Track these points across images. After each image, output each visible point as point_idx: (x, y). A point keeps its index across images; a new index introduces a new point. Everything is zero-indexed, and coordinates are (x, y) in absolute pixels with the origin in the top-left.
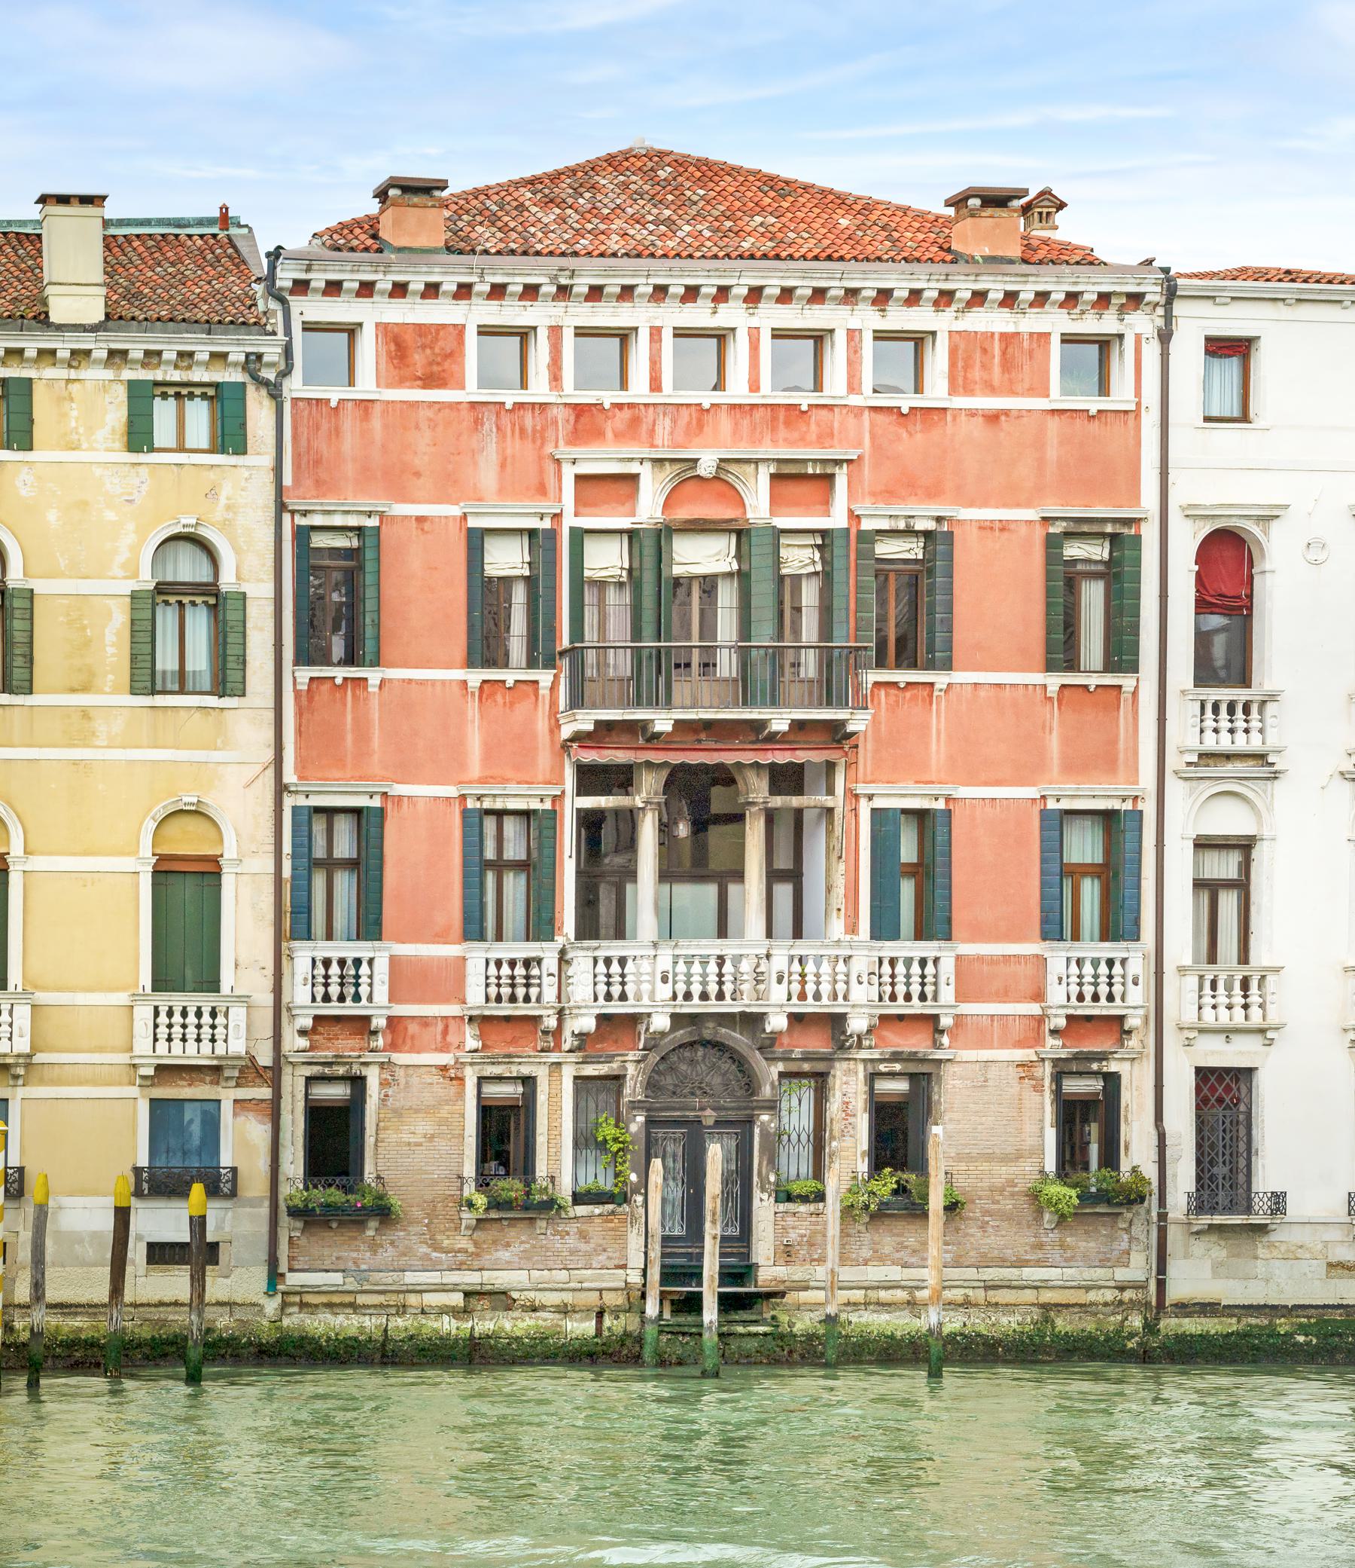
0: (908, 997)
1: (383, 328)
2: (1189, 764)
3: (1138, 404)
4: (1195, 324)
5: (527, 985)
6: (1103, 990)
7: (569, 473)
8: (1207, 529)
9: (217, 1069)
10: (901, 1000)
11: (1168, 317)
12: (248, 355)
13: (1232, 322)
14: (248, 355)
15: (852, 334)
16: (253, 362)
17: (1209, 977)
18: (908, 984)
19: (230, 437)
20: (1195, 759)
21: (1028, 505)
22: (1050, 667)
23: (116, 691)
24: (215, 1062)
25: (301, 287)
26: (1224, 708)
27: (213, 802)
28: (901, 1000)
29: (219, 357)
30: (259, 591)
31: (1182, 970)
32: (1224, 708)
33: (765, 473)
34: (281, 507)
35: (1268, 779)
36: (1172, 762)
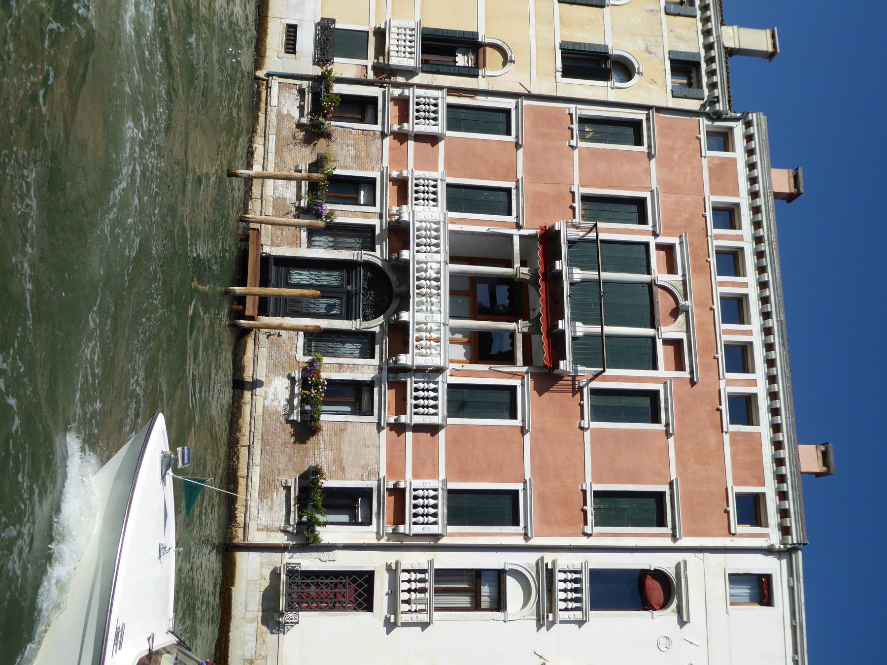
0: (416, 398)
1: (734, 160)
2: (547, 565)
3: (734, 535)
5: (424, 199)
6: (420, 510)
7: (675, 240)
8: (672, 573)
9: (383, 54)
10: (415, 394)
12: (718, 97)
14: (718, 97)
15: (754, 383)
16: (713, 101)
17: (427, 576)
18: (423, 398)
20: (550, 567)
21: (678, 473)
23: (561, 35)
24: (387, 51)
25: (748, 124)
26: (578, 585)
27: (509, 66)
28: (415, 394)
29: (713, 86)
31: (431, 562)
32: (578, 585)
33: (683, 336)
34: (647, 108)
35: (538, 615)
36: (549, 557)
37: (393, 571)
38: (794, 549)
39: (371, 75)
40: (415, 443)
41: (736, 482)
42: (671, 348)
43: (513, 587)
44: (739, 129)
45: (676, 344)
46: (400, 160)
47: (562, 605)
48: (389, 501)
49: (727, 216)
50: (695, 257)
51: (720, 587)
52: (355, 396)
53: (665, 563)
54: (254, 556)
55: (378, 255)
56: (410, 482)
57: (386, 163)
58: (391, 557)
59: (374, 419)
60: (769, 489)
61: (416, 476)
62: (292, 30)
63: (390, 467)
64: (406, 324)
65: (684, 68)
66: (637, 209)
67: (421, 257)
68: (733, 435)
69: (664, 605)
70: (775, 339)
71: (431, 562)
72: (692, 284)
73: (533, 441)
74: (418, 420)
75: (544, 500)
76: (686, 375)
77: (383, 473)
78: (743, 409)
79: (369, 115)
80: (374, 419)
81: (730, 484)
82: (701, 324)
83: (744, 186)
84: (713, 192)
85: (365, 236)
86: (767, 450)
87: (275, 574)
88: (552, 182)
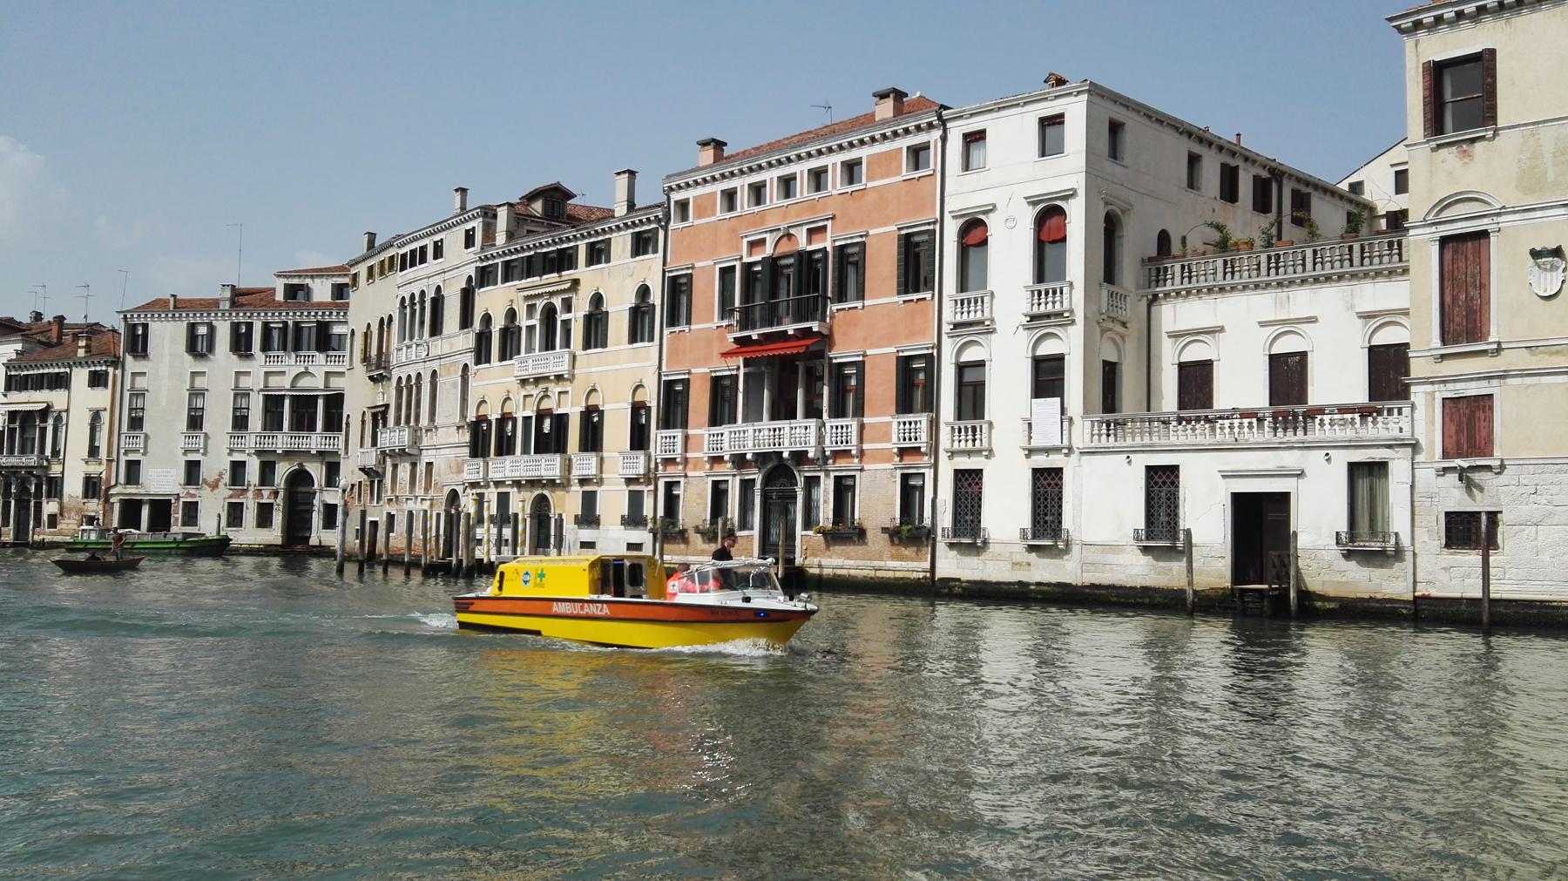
4: (956, 132)
8: (961, 221)
11: (945, 130)
13: (974, 125)
15: (834, 165)
16: (658, 220)
19: (655, 251)
22: (899, 293)
30: (658, 303)
31: (947, 424)
36: (946, 328)
37: (953, 454)
38: (940, 117)
39: (652, 487)
40: (872, 441)
41: (899, 173)
42: (814, 237)
43: (967, 357)
44: (675, 196)
45: (811, 232)
46: (698, 464)
47: (979, 314)
48: (908, 460)
49: (730, 196)
50: (755, 224)
51: (971, 178)
52: (844, 489)
53: (952, 229)
54: (939, 564)
55: (757, 476)
56: (893, 444)
57: (702, 474)
58: (943, 456)
59: (857, 474)
60: (904, 143)
61: (890, 440)
62: (631, 546)
63: (889, 460)
64: (792, 453)
65: (642, 244)
66: (727, 273)
67: (750, 444)
68: (868, 180)
69: (982, 223)
70: (803, 151)
71: (947, 424)
72: (771, 225)
73: (873, 346)
74: (854, 440)
75: (910, 335)
76: (829, 223)
77: (890, 466)
78: (851, 169)
79: (723, 486)
80: (857, 474)
81: (900, 178)
82: (798, 215)
83: (709, 189)
84: (714, 214)
85: (747, 486)
86: (878, 148)
87: (951, 546)
88: (707, 346)
